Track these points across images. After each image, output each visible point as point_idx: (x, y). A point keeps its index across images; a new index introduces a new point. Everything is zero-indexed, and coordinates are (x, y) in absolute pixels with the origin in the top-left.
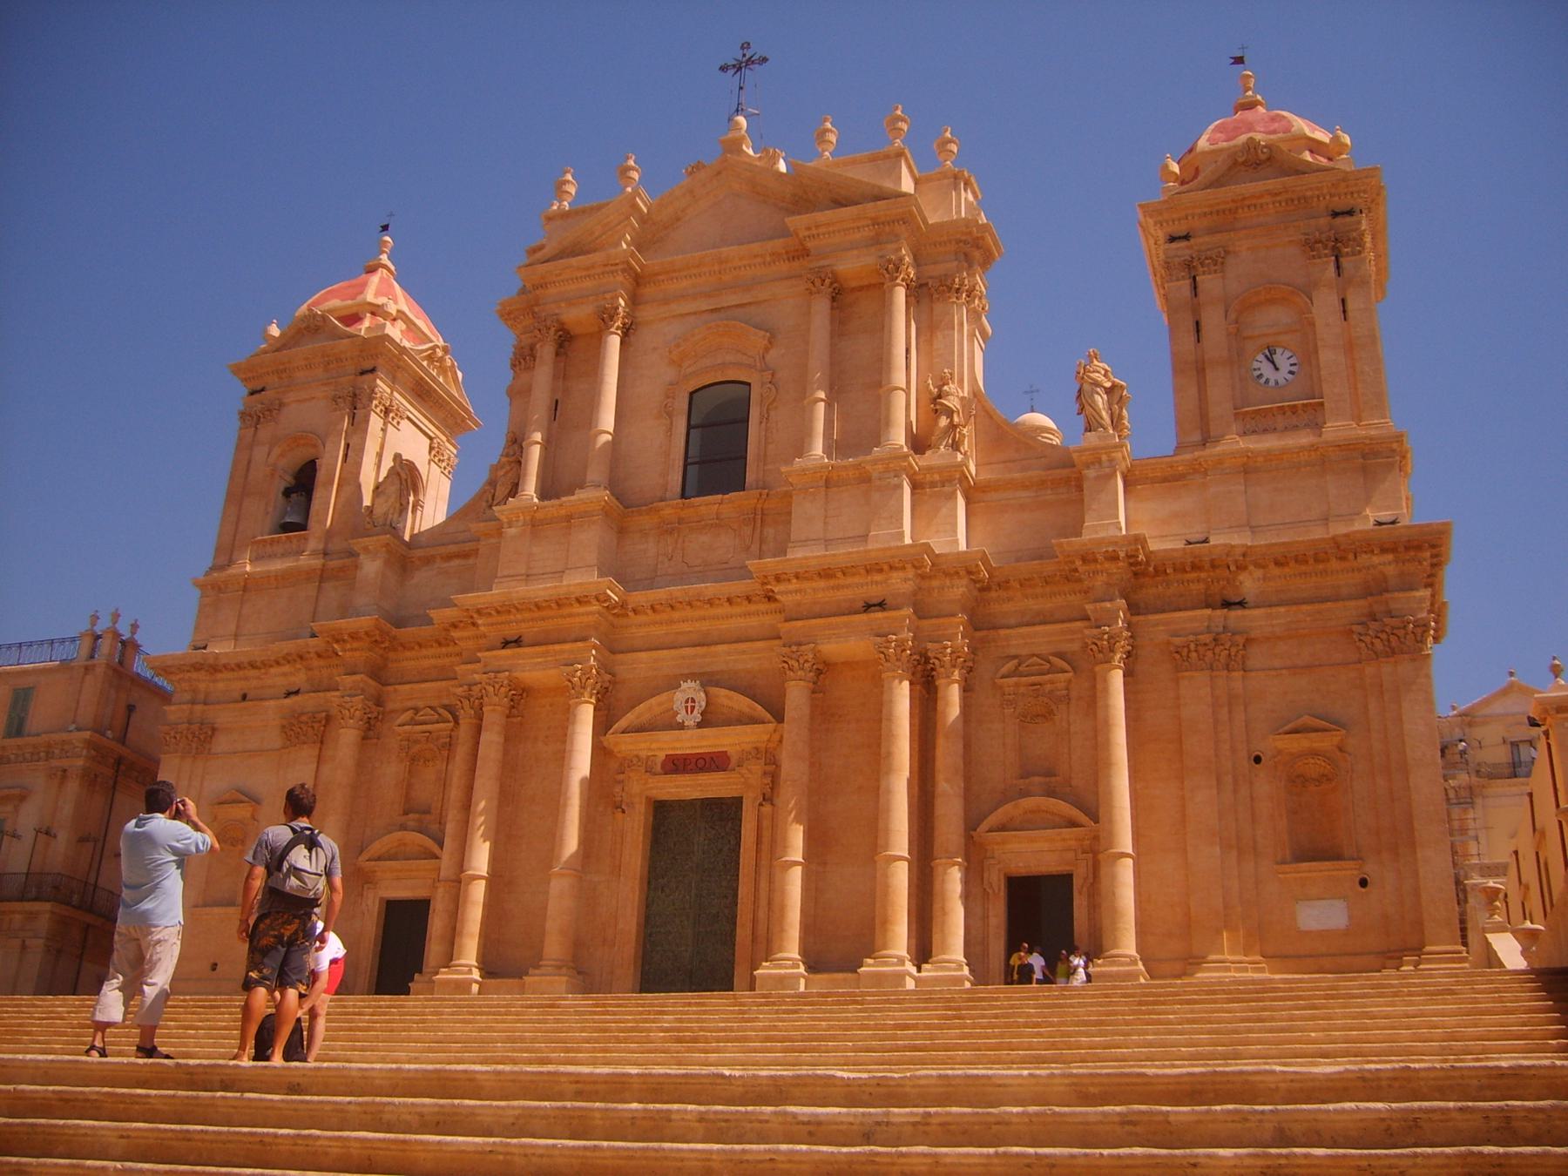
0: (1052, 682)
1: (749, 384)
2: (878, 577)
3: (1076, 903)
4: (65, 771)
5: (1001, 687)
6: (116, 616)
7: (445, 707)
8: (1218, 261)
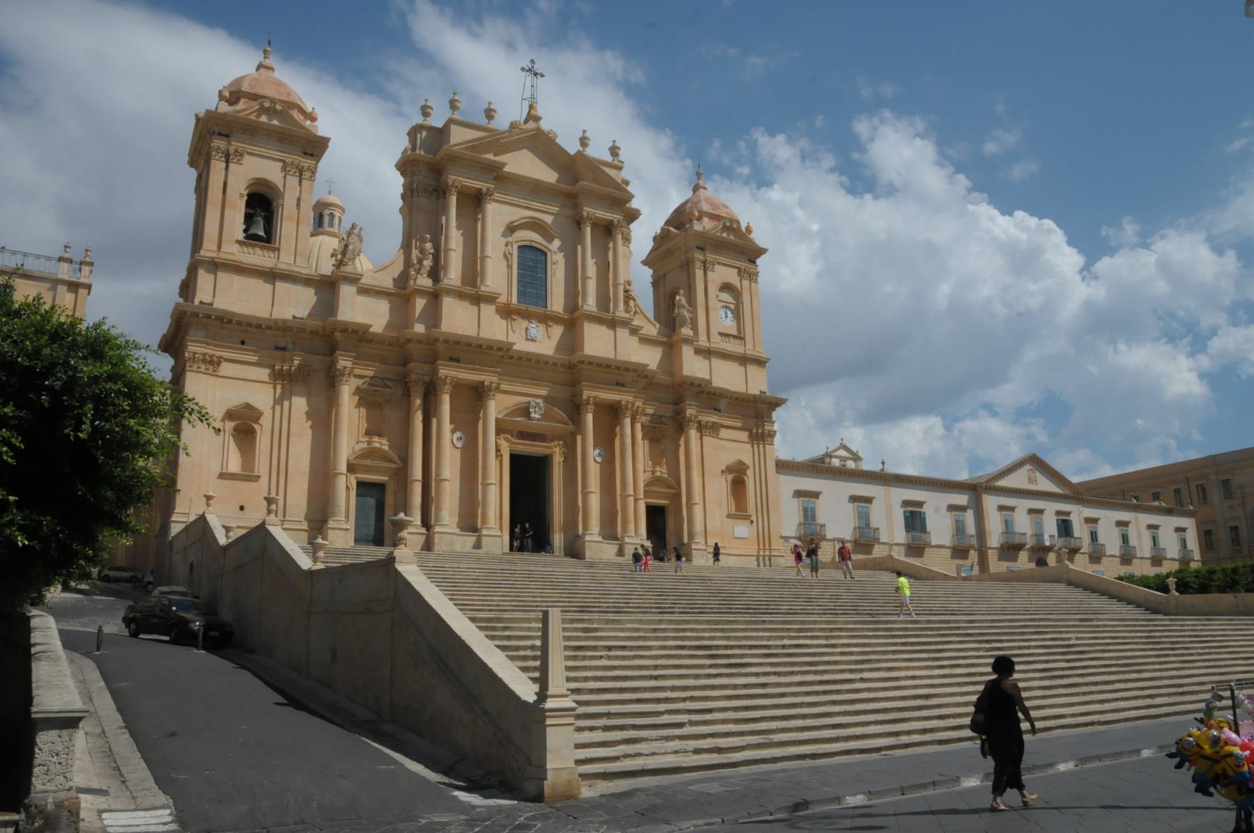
0: (661, 428)
2: (625, 373)
7: (388, 379)
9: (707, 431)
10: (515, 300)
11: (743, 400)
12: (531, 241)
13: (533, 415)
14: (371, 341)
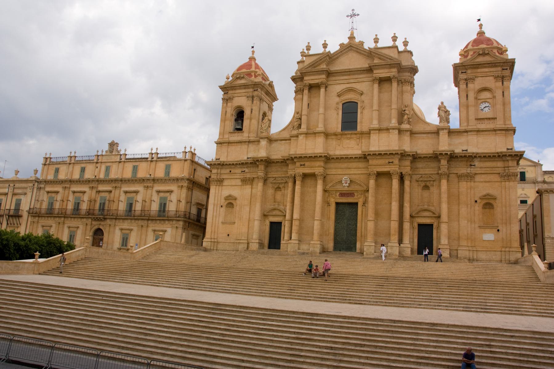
0: (430, 181)
1: (357, 103)
2: (392, 156)
3: (434, 231)
4: (182, 186)
5: (418, 181)
6: (191, 147)
8: (473, 79)
9: (463, 178)
10: (339, 130)
11: (489, 156)
12: (349, 99)
13: (344, 185)
14: (274, 162)
